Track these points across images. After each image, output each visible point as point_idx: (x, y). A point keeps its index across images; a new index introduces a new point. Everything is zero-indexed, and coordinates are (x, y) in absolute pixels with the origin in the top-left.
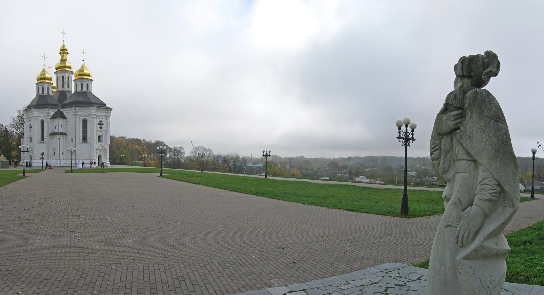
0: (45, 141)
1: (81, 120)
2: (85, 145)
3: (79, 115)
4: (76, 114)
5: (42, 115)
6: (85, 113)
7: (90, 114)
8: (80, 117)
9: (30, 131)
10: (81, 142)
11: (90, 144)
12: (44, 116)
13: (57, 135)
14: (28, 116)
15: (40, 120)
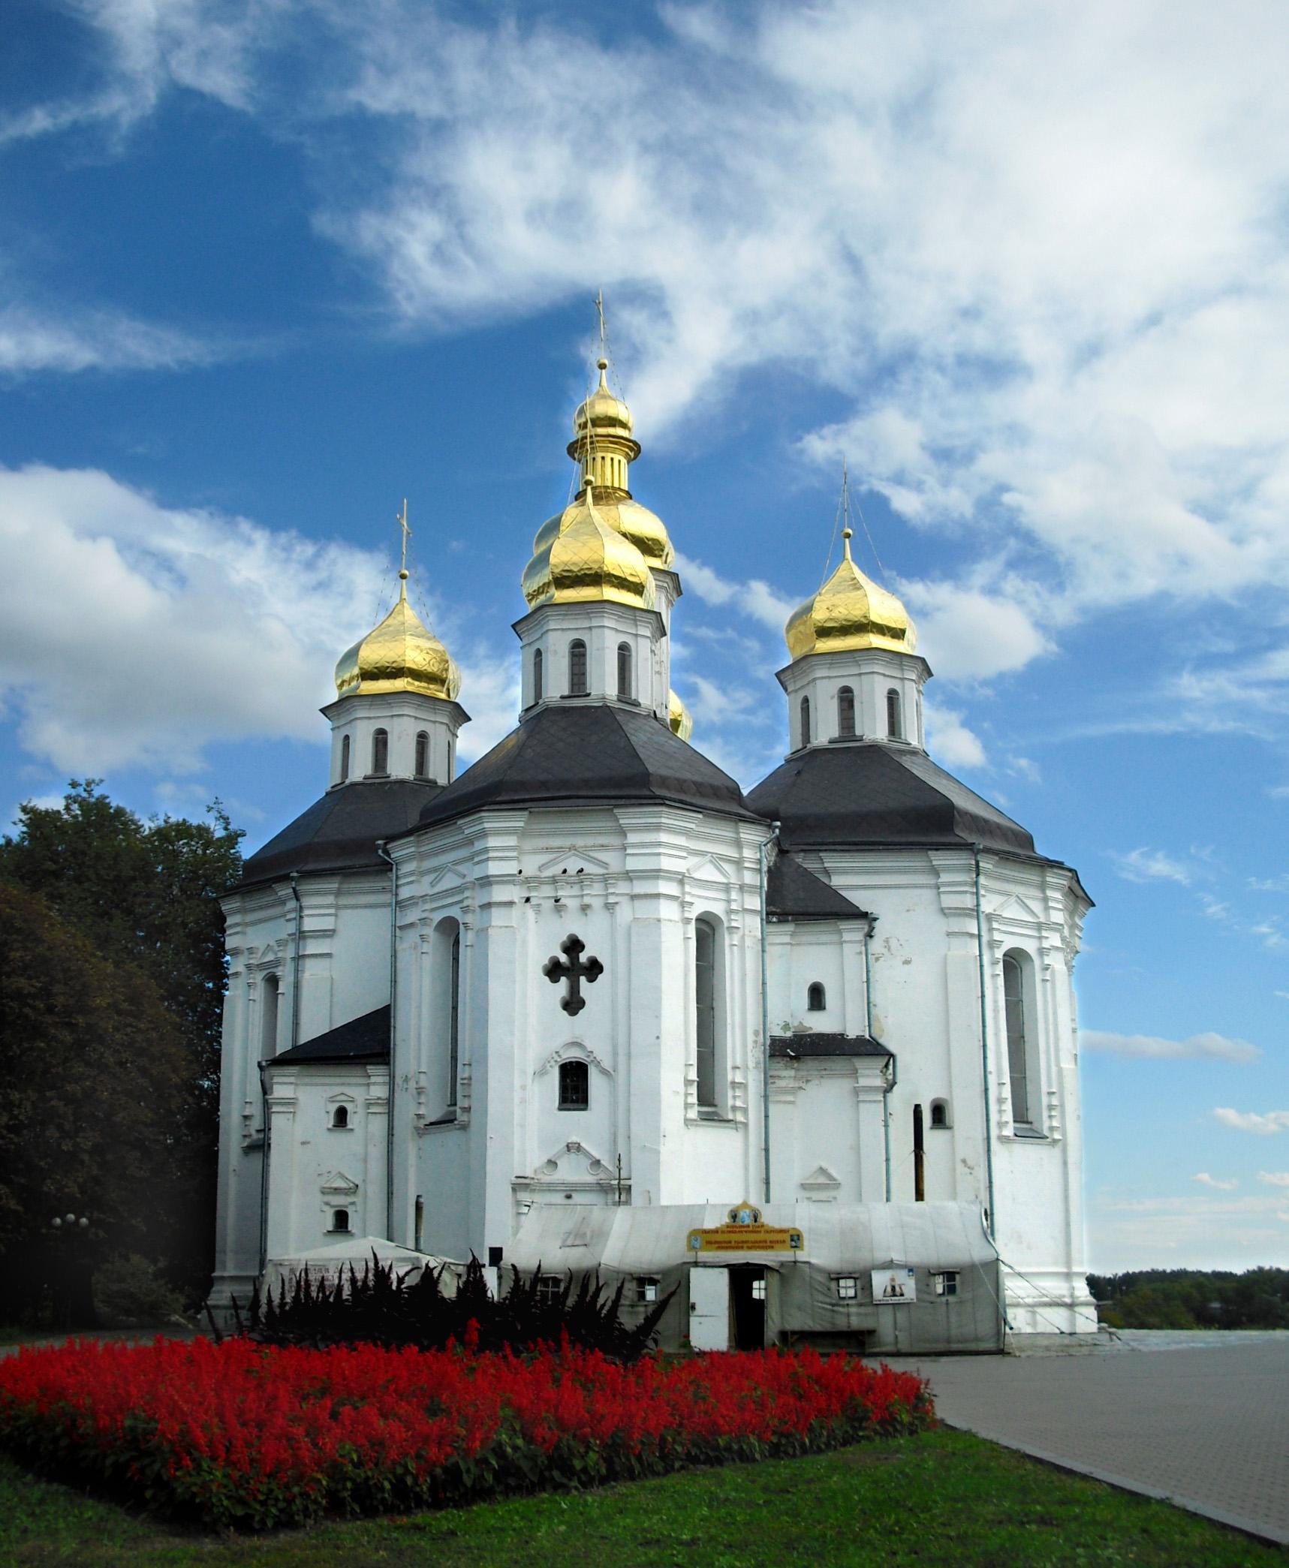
0: (730, 1102)
1: (999, 954)
2: (1028, 1153)
3: (990, 918)
4: (978, 905)
5: (708, 873)
6: (1013, 911)
7: (1042, 920)
8: (997, 936)
9: (573, 1004)
10: (1009, 1132)
11: (1056, 1152)
12: (727, 888)
13: (860, 1063)
14: (540, 869)
15: (693, 913)
